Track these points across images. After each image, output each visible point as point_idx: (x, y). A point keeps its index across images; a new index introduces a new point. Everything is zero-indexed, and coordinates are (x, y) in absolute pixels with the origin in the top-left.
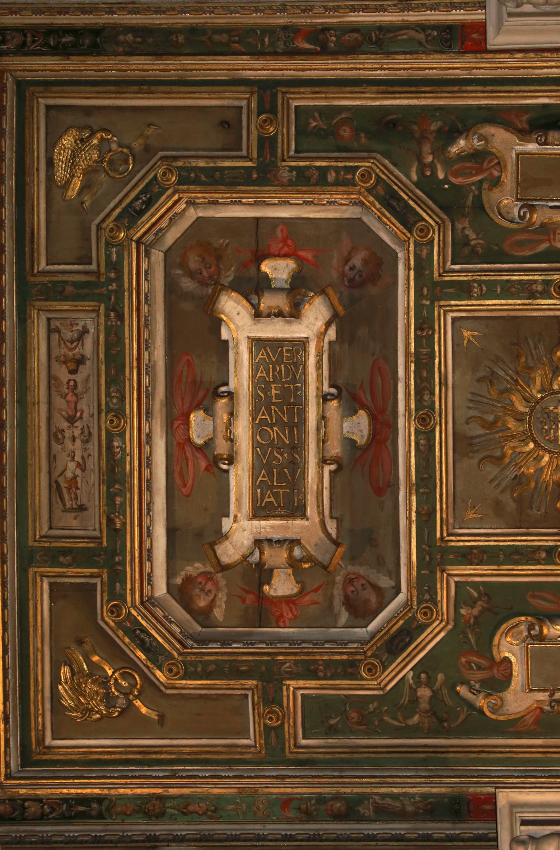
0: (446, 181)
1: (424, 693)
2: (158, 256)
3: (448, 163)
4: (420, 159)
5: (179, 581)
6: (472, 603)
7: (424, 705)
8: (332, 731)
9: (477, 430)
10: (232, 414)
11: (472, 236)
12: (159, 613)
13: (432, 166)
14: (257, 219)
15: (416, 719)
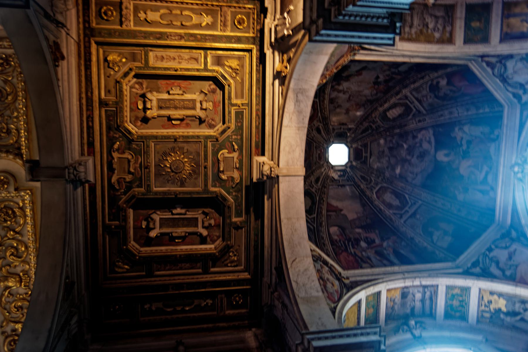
0: (124, 190)
1: (234, 194)
2: (142, 249)
3: (120, 189)
4: (119, 195)
5: (211, 243)
6: (216, 184)
7: (237, 194)
8: (242, 212)
9: (179, 183)
10: (176, 232)
11: (136, 184)
12: (218, 246)
13: (121, 192)
14: (134, 228)
15: (240, 196)
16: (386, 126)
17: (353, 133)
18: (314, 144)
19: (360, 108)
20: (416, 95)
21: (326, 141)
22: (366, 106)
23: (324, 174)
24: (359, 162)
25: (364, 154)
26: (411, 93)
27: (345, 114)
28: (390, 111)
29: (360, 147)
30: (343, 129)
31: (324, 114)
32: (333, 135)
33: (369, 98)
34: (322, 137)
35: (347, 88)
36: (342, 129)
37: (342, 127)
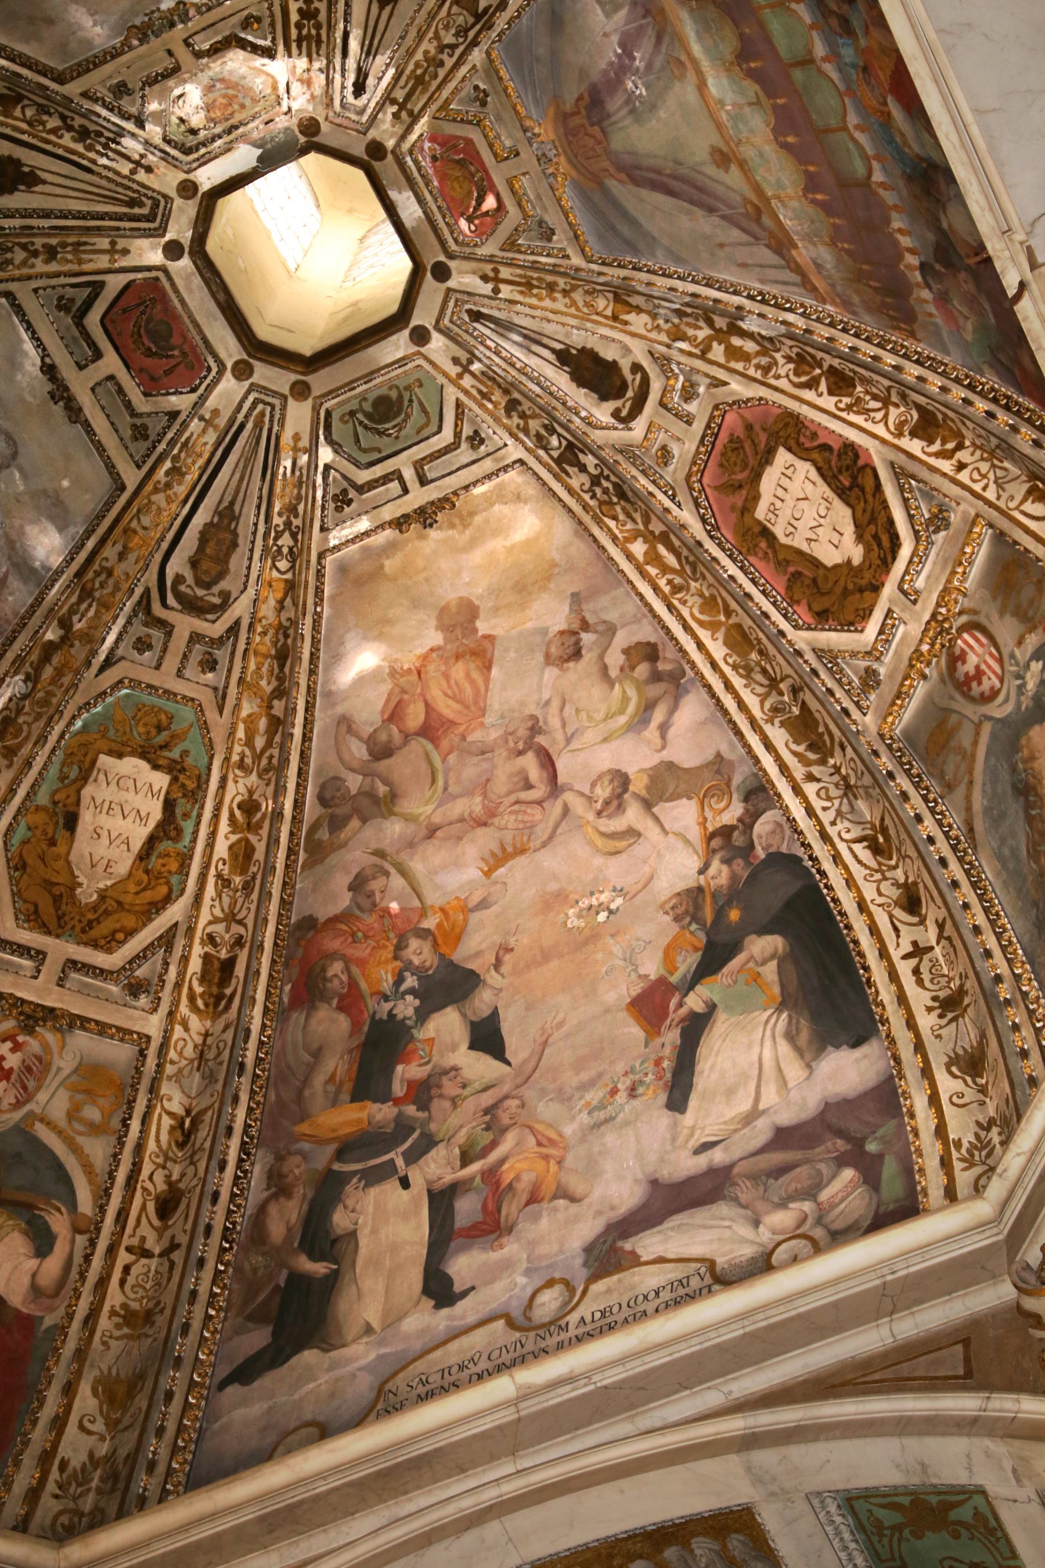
16: (91, 682)
17: (303, 481)
18: (577, 260)
19: (394, 714)
20: (81, 1040)
21: (477, 316)
22: (358, 751)
23: (354, 45)
24: (115, 283)
25: (111, 362)
26: (124, 1034)
27: (469, 611)
28: (157, 815)
29: (181, 402)
30: (397, 475)
31: (650, 538)
32: (451, 394)
33: (394, 829)
34: (532, 339)
35: (633, 833)
36: (409, 474)
37: (419, 497)
